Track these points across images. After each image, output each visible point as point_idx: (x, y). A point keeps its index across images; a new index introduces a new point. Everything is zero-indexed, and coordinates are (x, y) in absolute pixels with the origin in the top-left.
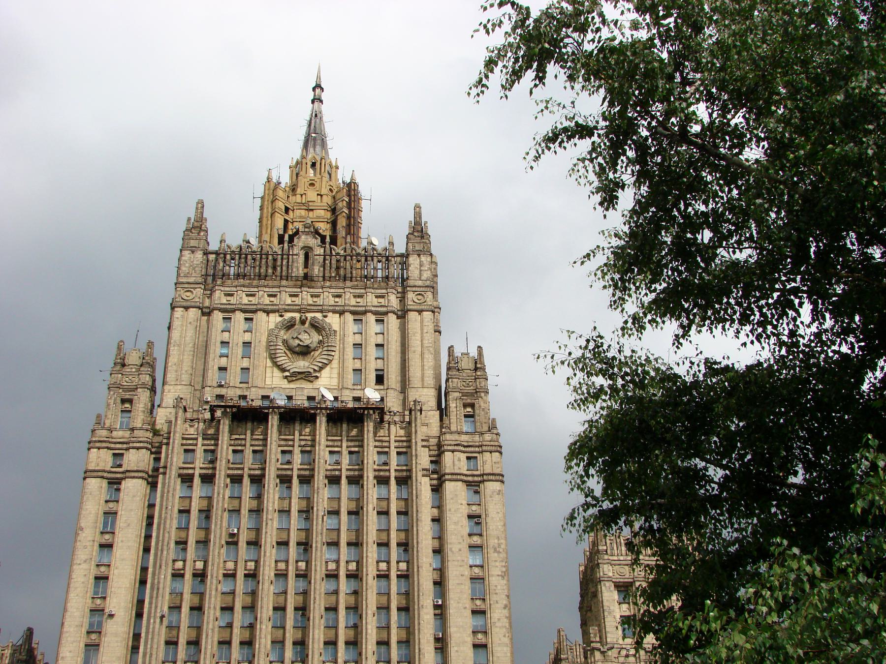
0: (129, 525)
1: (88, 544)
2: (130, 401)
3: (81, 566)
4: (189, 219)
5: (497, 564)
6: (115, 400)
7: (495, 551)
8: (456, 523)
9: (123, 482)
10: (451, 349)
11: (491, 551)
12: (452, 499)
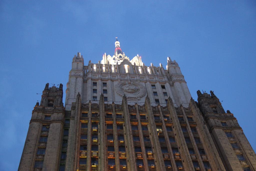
0: (55, 139)
1: (32, 146)
2: (53, 101)
3: (28, 155)
6: (46, 99)
7: (251, 155)
9: (51, 125)
10: (199, 92)
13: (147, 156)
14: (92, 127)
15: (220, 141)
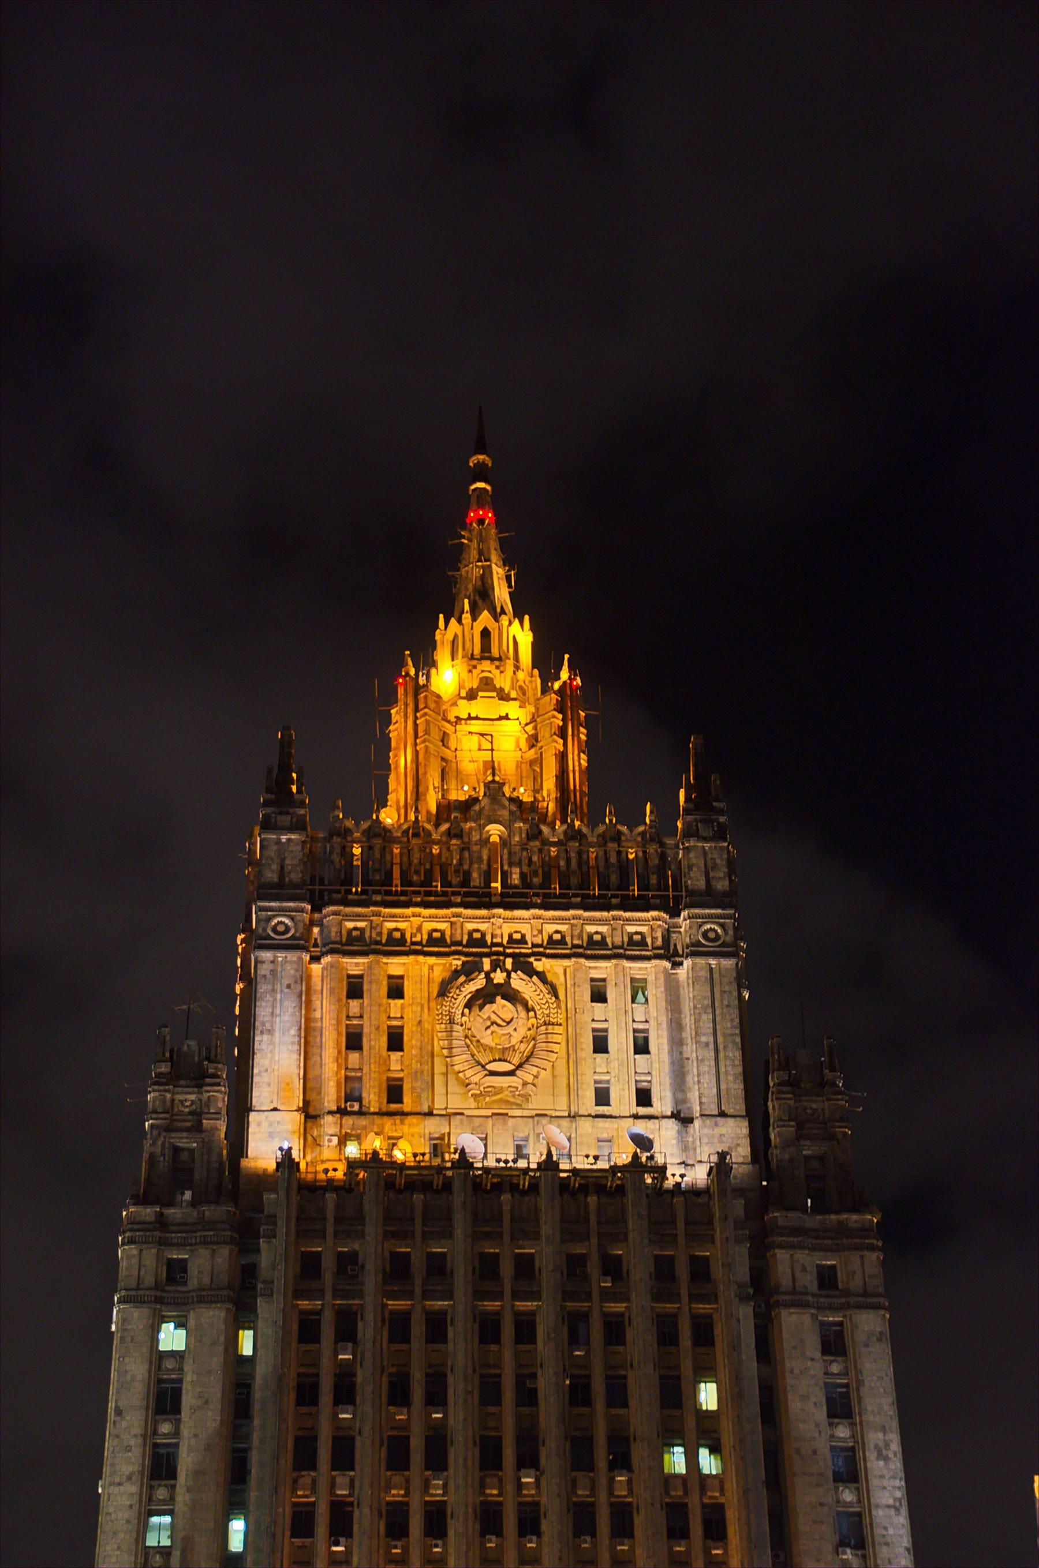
0: (206, 1402)
1: (132, 1443)
4: (270, 771)
5: (885, 1483)
7: (880, 1456)
8: (804, 1398)
11: (871, 1455)
12: (795, 1348)
13: (520, 1486)
14: (336, 1342)
15: (790, 1381)
